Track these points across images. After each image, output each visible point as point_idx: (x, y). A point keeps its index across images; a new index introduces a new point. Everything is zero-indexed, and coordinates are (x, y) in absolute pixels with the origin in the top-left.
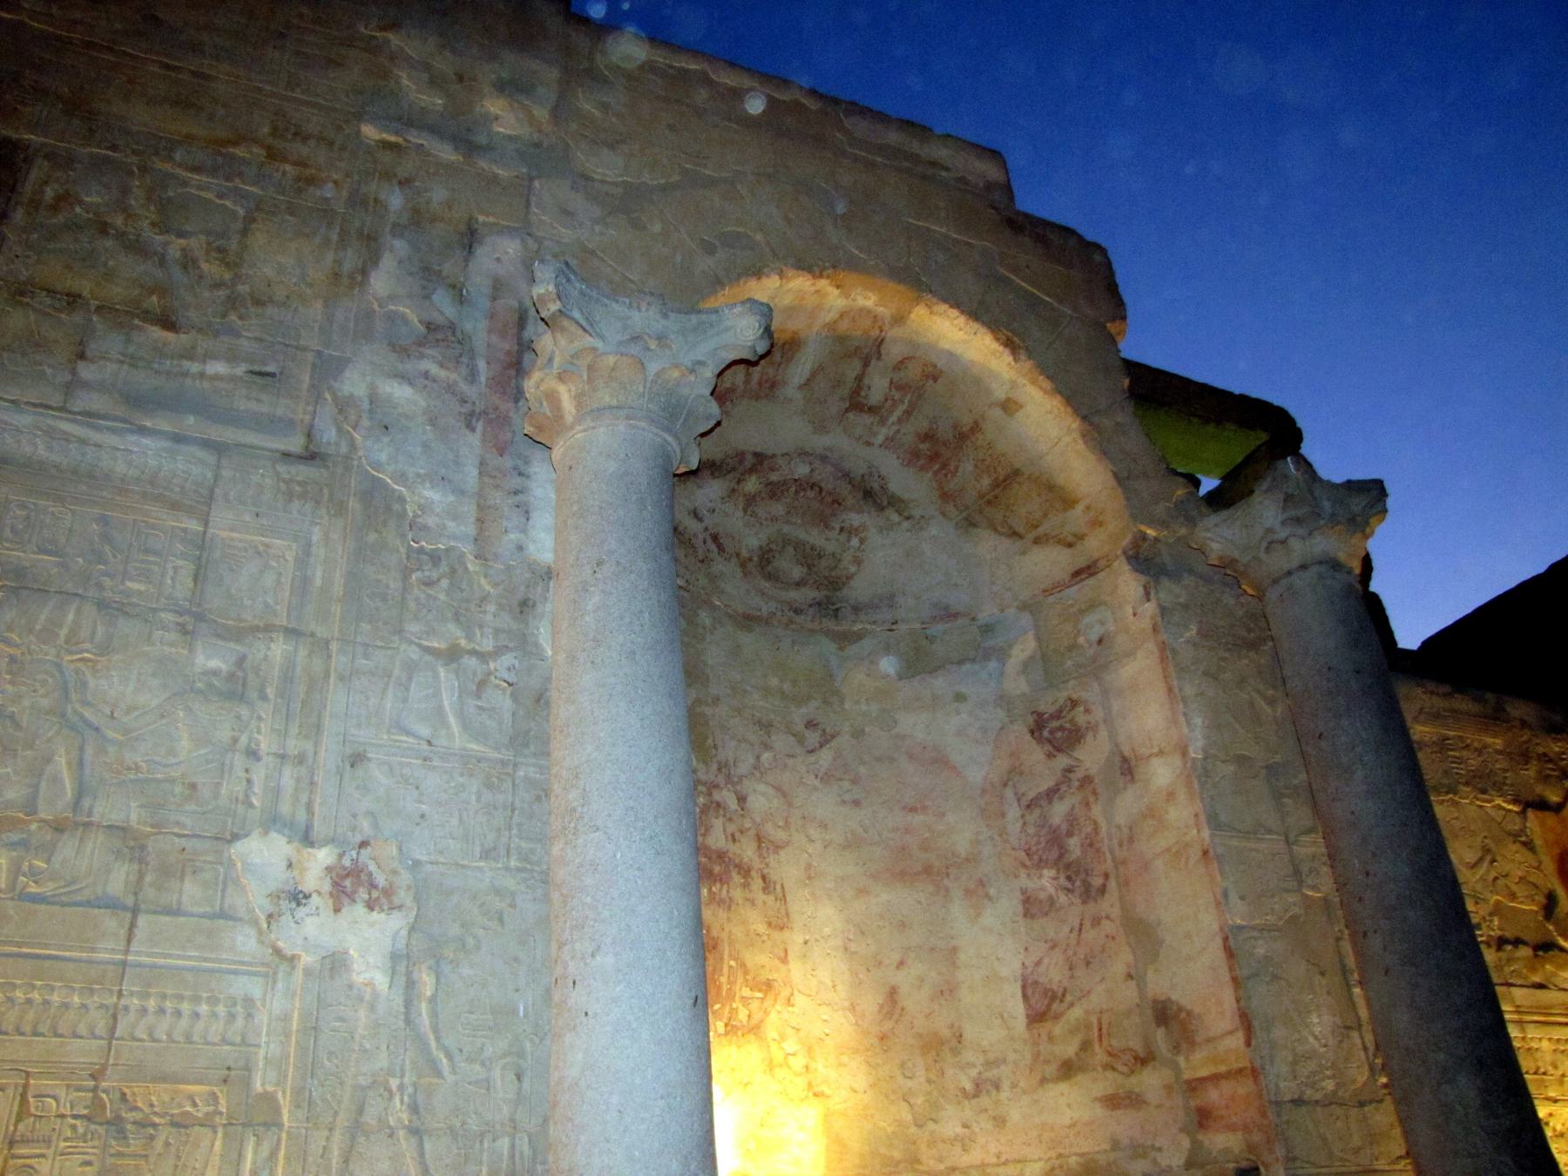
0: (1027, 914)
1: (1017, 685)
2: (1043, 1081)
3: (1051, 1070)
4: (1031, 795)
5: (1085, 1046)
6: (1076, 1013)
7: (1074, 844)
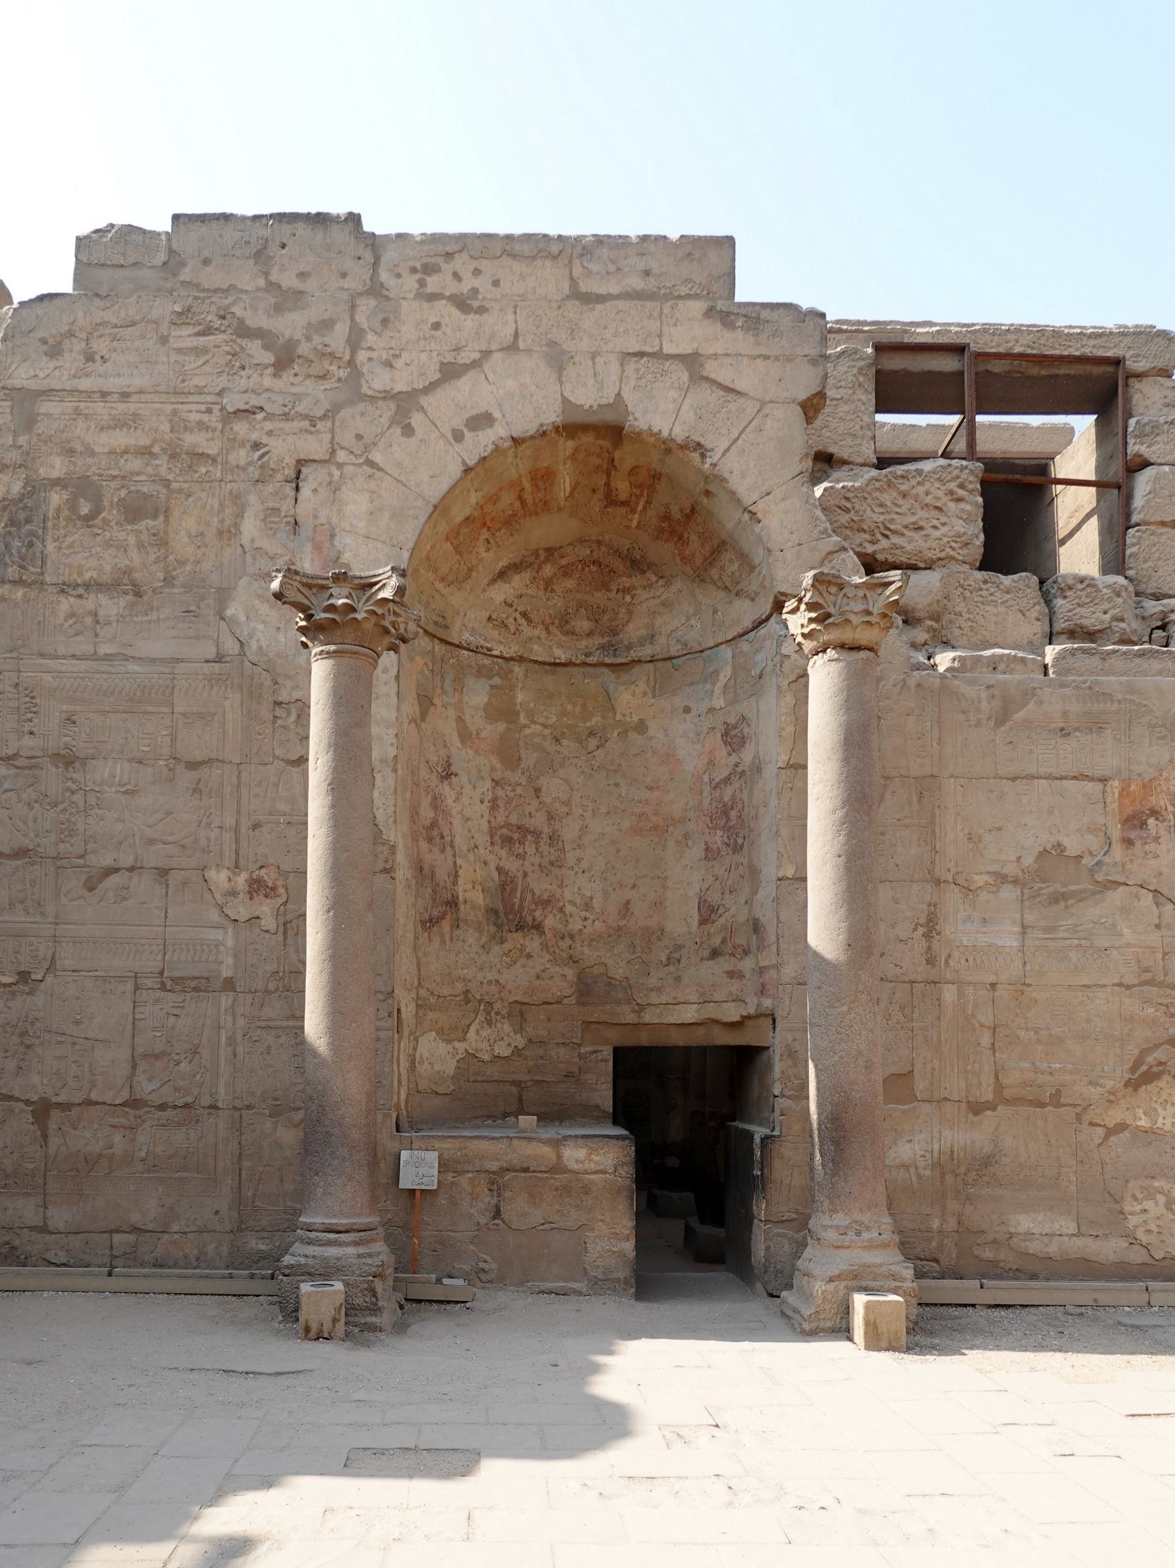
1: (719, 702)
2: (702, 959)
3: (706, 953)
4: (717, 780)
5: (724, 941)
6: (722, 920)
7: (733, 814)
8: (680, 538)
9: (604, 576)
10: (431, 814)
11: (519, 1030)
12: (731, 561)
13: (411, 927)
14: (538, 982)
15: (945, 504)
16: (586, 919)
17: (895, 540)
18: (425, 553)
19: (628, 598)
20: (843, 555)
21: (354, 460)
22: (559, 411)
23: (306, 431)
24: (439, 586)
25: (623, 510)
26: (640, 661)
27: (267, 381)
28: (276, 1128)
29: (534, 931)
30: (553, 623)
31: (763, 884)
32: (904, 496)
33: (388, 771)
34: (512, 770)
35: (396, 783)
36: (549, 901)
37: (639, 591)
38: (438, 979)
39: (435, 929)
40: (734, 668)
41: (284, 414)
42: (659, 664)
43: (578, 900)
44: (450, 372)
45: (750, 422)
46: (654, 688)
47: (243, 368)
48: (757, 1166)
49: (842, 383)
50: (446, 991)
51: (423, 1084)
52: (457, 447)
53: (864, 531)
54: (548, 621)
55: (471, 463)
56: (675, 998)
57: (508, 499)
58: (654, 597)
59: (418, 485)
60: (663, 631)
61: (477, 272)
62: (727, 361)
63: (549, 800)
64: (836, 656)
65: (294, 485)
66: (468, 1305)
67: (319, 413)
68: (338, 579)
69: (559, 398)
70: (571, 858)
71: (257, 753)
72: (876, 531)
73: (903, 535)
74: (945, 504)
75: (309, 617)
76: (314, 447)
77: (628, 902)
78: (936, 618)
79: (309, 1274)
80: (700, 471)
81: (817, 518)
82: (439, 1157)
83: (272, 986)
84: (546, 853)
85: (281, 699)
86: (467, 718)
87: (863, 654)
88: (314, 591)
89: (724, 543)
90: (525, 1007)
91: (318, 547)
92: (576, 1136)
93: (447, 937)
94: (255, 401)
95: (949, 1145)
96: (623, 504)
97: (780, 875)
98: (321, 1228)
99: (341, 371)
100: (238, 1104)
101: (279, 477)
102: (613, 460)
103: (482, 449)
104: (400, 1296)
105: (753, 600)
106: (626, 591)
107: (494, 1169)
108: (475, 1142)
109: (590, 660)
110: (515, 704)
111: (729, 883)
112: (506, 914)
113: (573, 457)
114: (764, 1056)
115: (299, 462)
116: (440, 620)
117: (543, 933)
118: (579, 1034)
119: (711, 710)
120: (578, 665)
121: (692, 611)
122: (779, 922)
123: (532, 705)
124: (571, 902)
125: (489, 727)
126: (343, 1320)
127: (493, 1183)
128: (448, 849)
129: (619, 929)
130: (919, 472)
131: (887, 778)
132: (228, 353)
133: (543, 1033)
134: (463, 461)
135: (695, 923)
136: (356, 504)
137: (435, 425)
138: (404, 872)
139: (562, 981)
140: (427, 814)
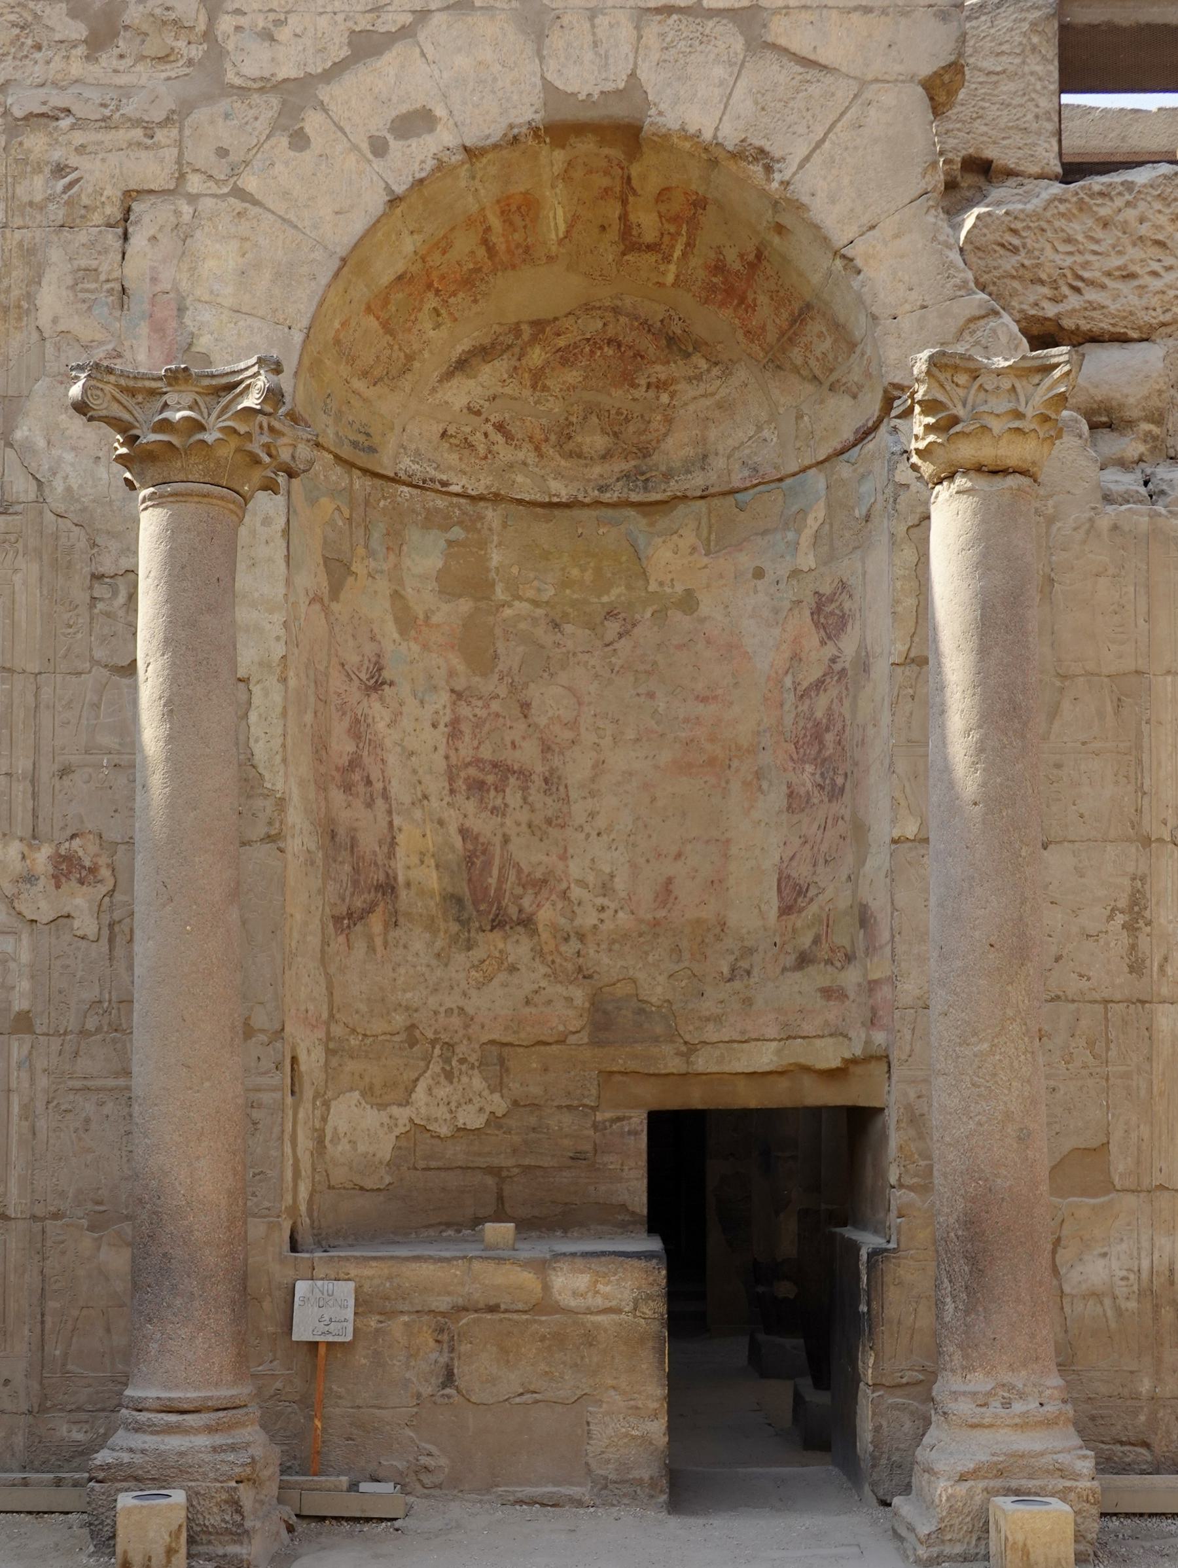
1: (807, 560)
3: (790, 960)
4: (805, 684)
7: (829, 737)
8: (742, 300)
9: (627, 364)
10: (350, 747)
11: (498, 1086)
12: (820, 335)
13: (315, 925)
14: (527, 1010)
15: (1170, 237)
16: (603, 909)
17: (1091, 295)
18: (333, 334)
19: (665, 398)
20: (993, 323)
21: (215, 189)
22: (539, 104)
23: (139, 144)
24: (359, 385)
26: (685, 497)
27: (77, 68)
28: (99, 1248)
29: (520, 929)
30: (547, 440)
31: (873, 850)
32: (1105, 225)
33: (272, 681)
34: (484, 675)
35: (285, 698)
36: (545, 881)
37: (681, 386)
38: (363, 1008)
39: (359, 928)
40: (829, 506)
41: (103, 120)
42: (716, 502)
43: (591, 879)
44: (365, 46)
45: (843, 114)
46: (708, 540)
47: (38, 47)
48: (864, 1298)
49: (1005, 47)
50: (378, 1026)
51: (339, 1176)
52: (378, 164)
53: (1042, 282)
54: (539, 435)
55: (399, 189)
57: (465, 244)
59: (315, 227)
60: (720, 448)
62: (805, 16)
64: (969, 484)
65: (120, 231)
66: (397, 1524)
67: (158, 115)
68: (176, 379)
69: (539, 83)
70: (579, 810)
71: (65, 656)
72: (1061, 282)
73: (1103, 287)
74: (1170, 237)
75: (131, 440)
76: (151, 170)
77: (670, 881)
78: (1157, 418)
79: (137, 1479)
80: (764, 193)
81: (951, 265)
82: (356, 1291)
83: (91, 1025)
84: (538, 806)
85: (101, 570)
86: (409, 592)
87: (1012, 481)
88: (140, 398)
89: (809, 306)
90: (506, 1050)
91: (158, 329)
92: (573, 1255)
93: (378, 941)
94: (58, 100)
95: (1166, 1260)
96: (650, 248)
97: (896, 834)
98: (156, 1405)
99: (193, 46)
100: (39, 1210)
101: (97, 218)
103: (416, 167)
104: (288, 1512)
105: (855, 397)
106: (660, 386)
107: (443, 1308)
108: (414, 1265)
109: (606, 497)
110: (488, 570)
111: (824, 848)
112: (475, 903)
113: (566, 176)
114: (878, 1124)
115: (127, 193)
116: (361, 438)
117: (534, 932)
118: (594, 1092)
119: (795, 573)
120: (588, 505)
121: (764, 416)
122: (894, 909)
123: (515, 570)
124: (582, 883)
125: (446, 607)
126: (183, 1551)
127: (442, 1331)
128: (380, 802)
129: (656, 923)
130: (1129, 186)
131: (1064, 677)
132: (14, 25)
133: (535, 1090)
134: (388, 188)
135: (773, 913)
136: (218, 257)
137: (341, 129)
138: (301, 838)
139: (566, 1008)
140: (342, 746)
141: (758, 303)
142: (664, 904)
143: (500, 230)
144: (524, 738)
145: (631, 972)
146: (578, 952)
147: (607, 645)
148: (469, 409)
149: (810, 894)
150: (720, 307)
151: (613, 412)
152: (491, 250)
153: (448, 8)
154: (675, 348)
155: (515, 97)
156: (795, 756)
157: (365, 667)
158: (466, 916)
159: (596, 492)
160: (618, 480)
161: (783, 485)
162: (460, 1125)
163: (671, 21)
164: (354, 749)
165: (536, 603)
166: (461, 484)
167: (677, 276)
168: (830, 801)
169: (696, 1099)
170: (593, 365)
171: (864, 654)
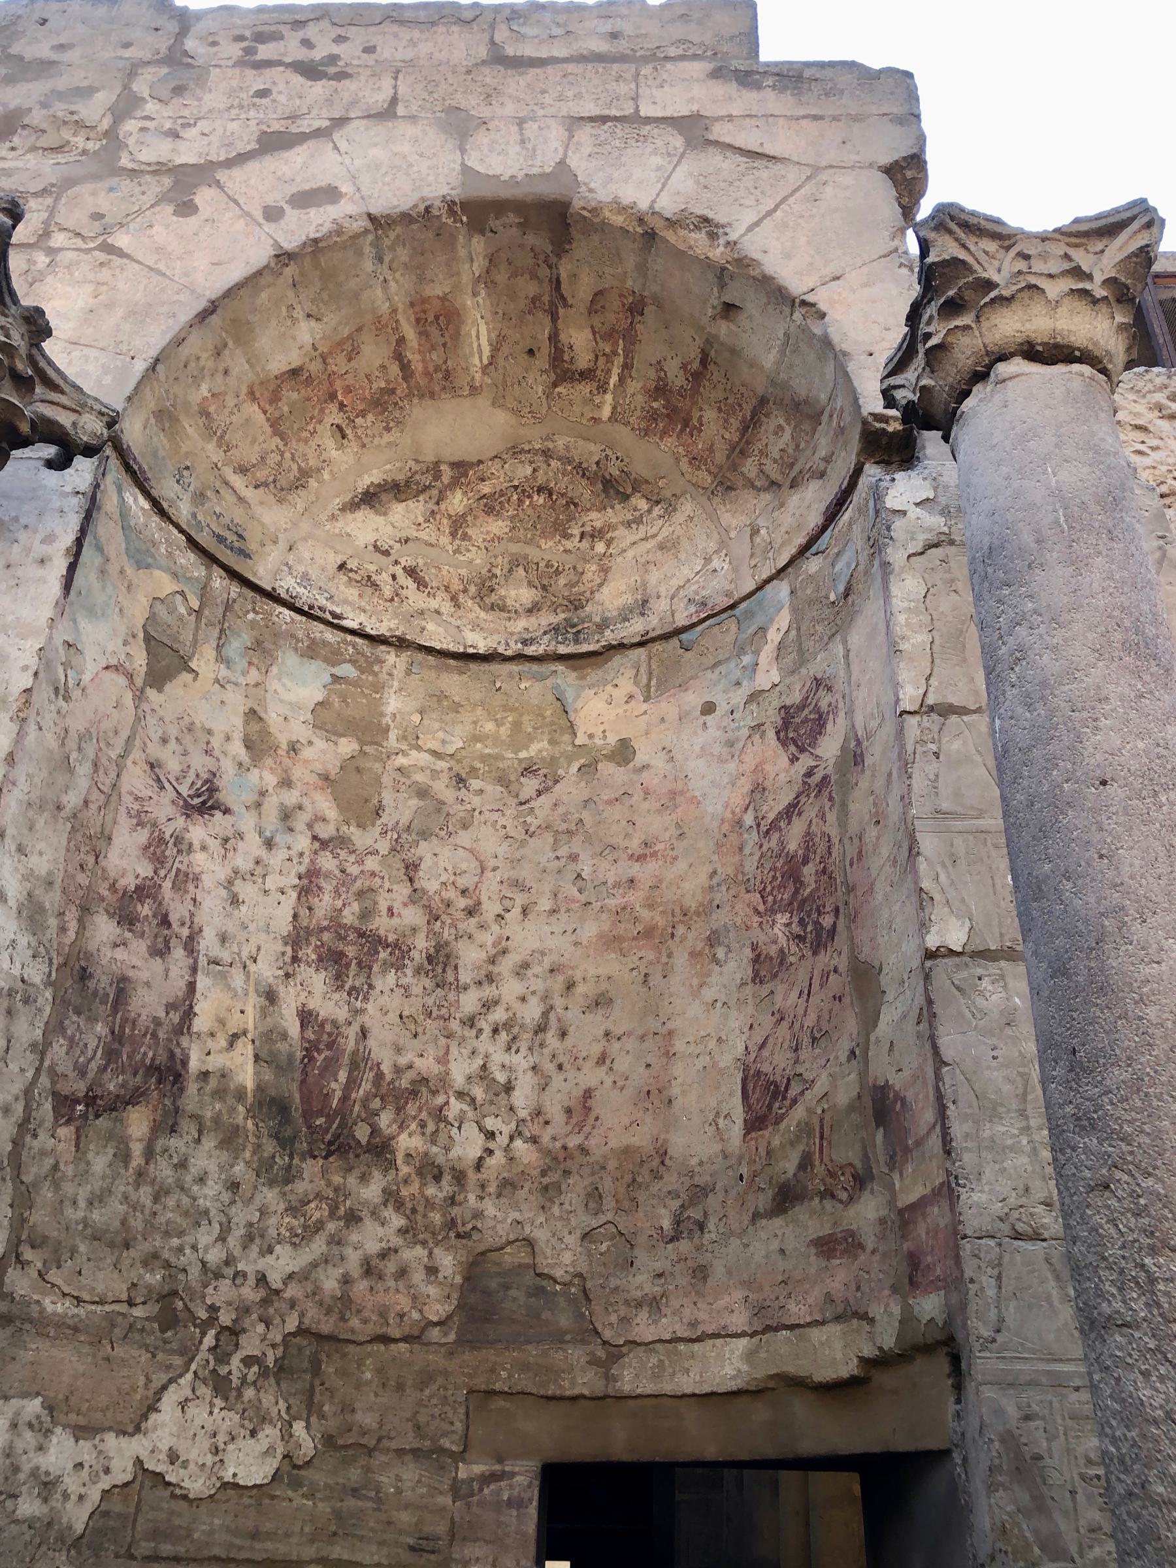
0: (757, 978)
1: (768, 675)
2: (756, 1216)
3: (763, 1201)
4: (771, 816)
5: (805, 1163)
6: (799, 1112)
8: (686, 423)
9: (560, 512)
19: (600, 547)
22: (455, 183)
25: (585, 388)
30: (465, 591)
39: (103, 1123)
40: (795, 610)
42: (658, 647)
46: (648, 685)
52: (268, 227)
54: (456, 586)
56: (693, 1325)
58: (646, 539)
60: (663, 590)
61: (340, 39)
63: (432, 886)
77: (588, 1094)
96: (586, 375)
102: (558, 282)
103: (312, 229)
106: (596, 535)
109: (530, 650)
110: (382, 715)
111: (810, 1021)
112: (308, 1115)
119: (754, 697)
121: (712, 546)
125: (320, 744)
128: (178, 953)
135: (738, 1128)
141: (705, 420)
142: (580, 1126)
143: (415, 344)
144: (405, 905)
145: (527, 1230)
146: (452, 1198)
147: (521, 804)
148: (375, 546)
149: (792, 1093)
150: (661, 438)
151: (542, 564)
152: (405, 367)
153: (369, 116)
154: (612, 491)
155: (431, 178)
156: (761, 908)
157: (189, 781)
158: (288, 1132)
159: (520, 646)
160: (545, 633)
161: (737, 612)
162: (228, 1477)
163: (605, 127)
164: (151, 874)
165: (435, 754)
166: (358, 621)
167: (614, 408)
168: (815, 953)
169: (619, 1442)
170: (522, 516)
171: (853, 744)
